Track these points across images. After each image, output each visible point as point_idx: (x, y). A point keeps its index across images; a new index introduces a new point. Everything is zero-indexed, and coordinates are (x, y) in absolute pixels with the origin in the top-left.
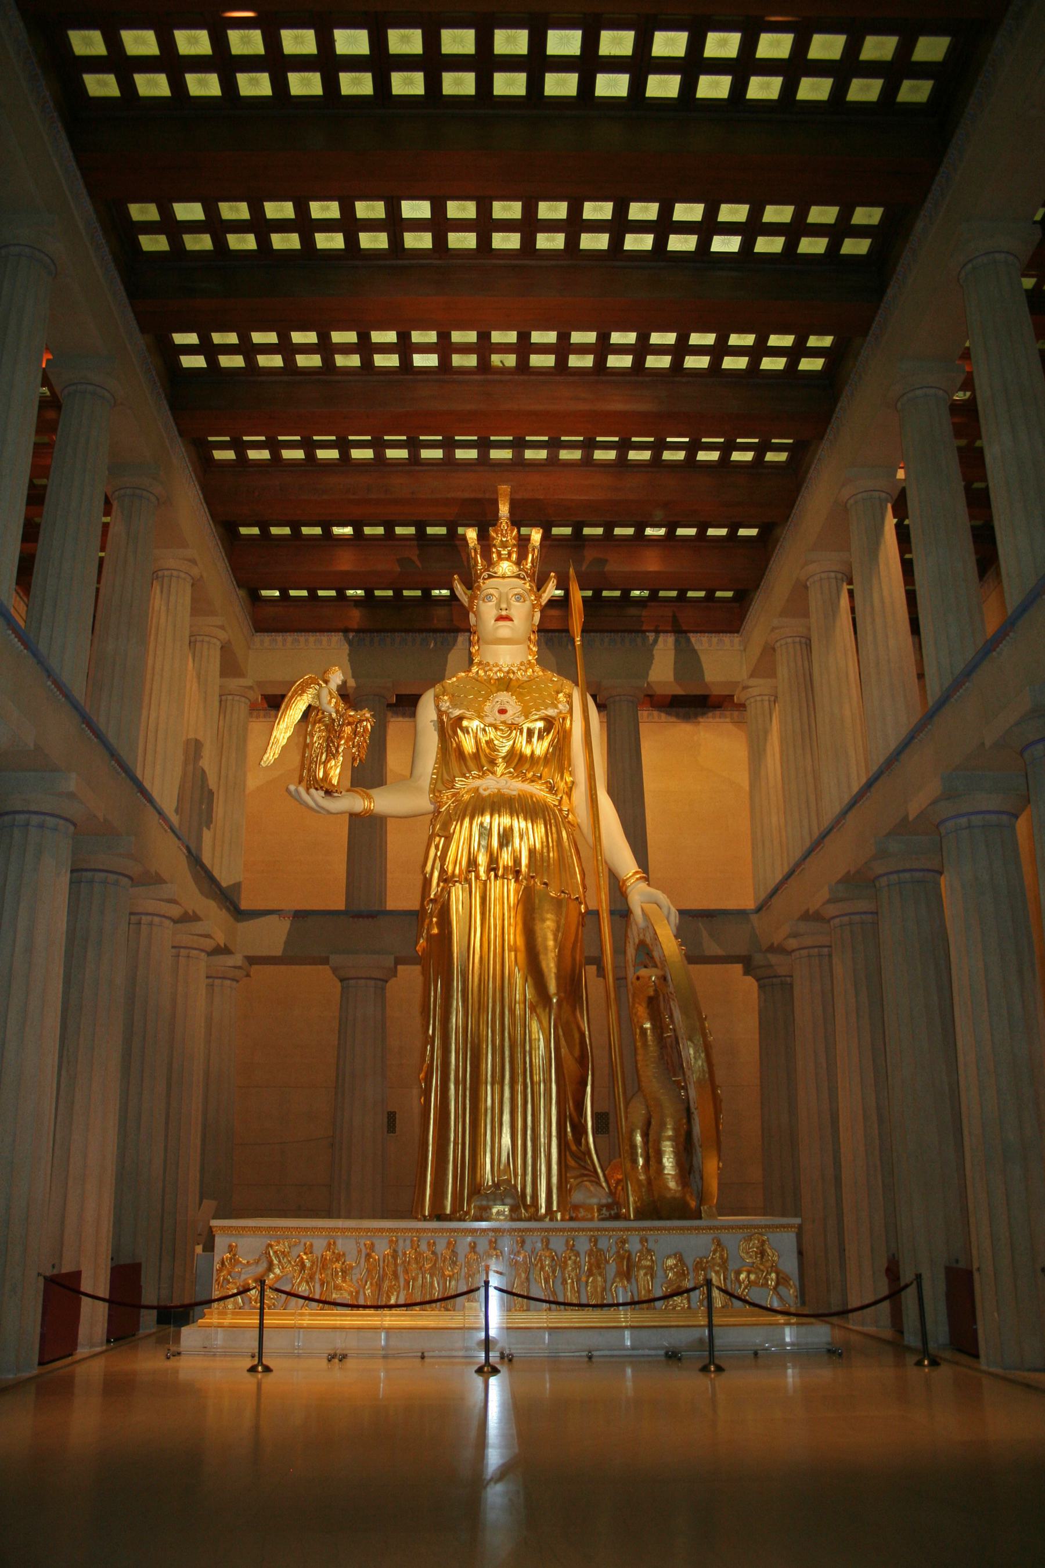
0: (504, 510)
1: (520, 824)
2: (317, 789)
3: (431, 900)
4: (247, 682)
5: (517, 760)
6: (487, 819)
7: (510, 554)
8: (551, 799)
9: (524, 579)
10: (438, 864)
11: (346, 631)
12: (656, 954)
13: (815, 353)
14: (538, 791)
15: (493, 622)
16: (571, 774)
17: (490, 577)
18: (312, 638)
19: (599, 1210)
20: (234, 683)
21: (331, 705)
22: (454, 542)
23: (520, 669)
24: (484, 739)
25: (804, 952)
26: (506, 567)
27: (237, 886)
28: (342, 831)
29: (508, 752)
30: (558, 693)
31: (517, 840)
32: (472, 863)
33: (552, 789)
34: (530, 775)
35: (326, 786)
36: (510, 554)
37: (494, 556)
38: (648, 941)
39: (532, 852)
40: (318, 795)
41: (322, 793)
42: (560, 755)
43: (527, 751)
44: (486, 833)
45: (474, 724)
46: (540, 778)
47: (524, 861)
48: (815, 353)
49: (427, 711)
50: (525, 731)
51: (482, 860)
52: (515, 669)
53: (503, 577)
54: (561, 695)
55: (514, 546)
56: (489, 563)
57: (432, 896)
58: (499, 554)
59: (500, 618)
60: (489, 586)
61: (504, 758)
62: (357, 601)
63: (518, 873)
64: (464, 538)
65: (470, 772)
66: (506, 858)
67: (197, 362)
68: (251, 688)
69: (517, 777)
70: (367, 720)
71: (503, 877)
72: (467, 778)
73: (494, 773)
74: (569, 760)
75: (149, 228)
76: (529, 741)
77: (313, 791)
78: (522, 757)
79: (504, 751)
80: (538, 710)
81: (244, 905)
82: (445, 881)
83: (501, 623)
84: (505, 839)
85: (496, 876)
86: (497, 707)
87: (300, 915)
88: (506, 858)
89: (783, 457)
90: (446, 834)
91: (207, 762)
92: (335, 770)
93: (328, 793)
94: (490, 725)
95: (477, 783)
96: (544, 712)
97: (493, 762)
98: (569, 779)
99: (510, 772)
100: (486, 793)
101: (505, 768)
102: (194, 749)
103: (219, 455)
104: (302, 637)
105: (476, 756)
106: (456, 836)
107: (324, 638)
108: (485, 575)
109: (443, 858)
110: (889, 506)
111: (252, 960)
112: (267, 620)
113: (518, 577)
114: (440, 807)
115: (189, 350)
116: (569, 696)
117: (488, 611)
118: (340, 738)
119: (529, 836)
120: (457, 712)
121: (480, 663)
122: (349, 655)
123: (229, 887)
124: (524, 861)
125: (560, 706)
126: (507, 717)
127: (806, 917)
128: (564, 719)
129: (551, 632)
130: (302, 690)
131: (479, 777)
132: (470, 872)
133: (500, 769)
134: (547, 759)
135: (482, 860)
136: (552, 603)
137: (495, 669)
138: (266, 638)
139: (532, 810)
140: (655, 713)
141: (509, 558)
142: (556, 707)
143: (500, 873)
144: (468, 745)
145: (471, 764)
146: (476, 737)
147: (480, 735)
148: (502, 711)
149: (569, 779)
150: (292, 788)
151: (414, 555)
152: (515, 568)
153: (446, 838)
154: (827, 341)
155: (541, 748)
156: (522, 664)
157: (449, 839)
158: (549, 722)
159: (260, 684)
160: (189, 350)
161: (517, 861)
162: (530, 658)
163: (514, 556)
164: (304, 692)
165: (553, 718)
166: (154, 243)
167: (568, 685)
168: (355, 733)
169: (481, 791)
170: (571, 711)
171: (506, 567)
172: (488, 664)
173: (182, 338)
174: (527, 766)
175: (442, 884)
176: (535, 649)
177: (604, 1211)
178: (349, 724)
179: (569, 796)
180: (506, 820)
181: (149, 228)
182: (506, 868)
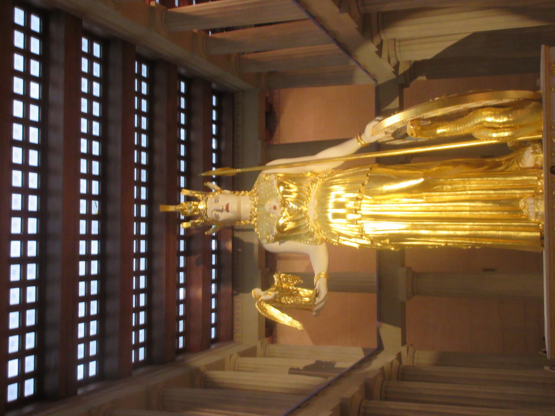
0: (172, 208)
1: (332, 199)
2: (315, 301)
3: (372, 243)
4: (258, 344)
5: (299, 200)
6: (330, 216)
7: (194, 205)
8: (320, 182)
9: (207, 198)
10: (352, 240)
11: (233, 295)
12: (399, 127)
13: (91, 47)
14: (315, 189)
15: (229, 213)
16: (307, 173)
17: (206, 215)
18: (236, 311)
19: (537, 153)
20: (259, 351)
21: (270, 294)
22: (188, 237)
23: (253, 200)
24: (289, 217)
25: (398, 55)
26: (201, 206)
27: (365, 350)
28: (336, 294)
29: (295, 204)
30: (265, 180)
31: (341, 200)
32: (353, 222)
33: (314, 182)
34: (307, 193)
35: (314, 296)
36: (194, 205)
37: (196, 213)
38: (392, 131)
39: (347, 191)
40: (318, 300)
43: (294, 195)
44: (336, 216)
45: (281, 222)
46: (309, 188)
47: (352, 195)
48: (91, 47)
49: (275, 247)
50: (285, 196)
51: (351, 216)
52: (253, 202)
53: (206, 209)
54: (266, 179)
55: (191, 203)
56: (200, 216)
58: (195, 210)
59: (227, 210)
60: (211, 215)
61: (299, 207)
62: (218, 289)
63: (357, 199)
64: (187, 230)
65: (306, 224)
66: (351, 205)
67: (93, 366)
68: (262, 343)
69: (308, 199)
70: (279, 276)
71: (360, 207)
72: (309, 226)
73: (306, 212)
74: (299, 174)
75: (21, 389)
76: (290, 193)
77: (316, 303)
78: (299, 197)
79: (295, 207)
81: (375, 346)
82: (362, 236)
83: (230, 209)
84: (340, 205)
85: (359, 210)
86: (272, 210)
87: (381, 318)
88: (351, 205)
89: (144, 68)
91: (301, 364)
92: (305, 293)
93: (317, 295)
94: (282, 213)
95: (311, 219)
96: (275, 186)
97: (301, 212)
98: (309, 174)
99: (306, 203)
100: (317, 216)
101: (304, 205)
102: (294, 371)
103: (142, 357)
104: (236, 316)
106: (339, 231)
107: (236, 305)
108: (205, 218)
109: (350, 237)
110: (169, 10)
111: (404, 343)
112: (227, 335)
113: (206, 201)
114: (323, 239)
115: (86, 370)
116: (267, 175)
117: (223, 216)
118: (289, 289)
119: (339, 192)
120: (275, 231)
121: (251, 221)
123: (365, 354)
125: (272, 179)
126: (278, 205)
127: (379, 53)
128: (278, 177)
129: (235, 184)
130: (264, 309)
131: (308, 219)
133: (304, 209)
134: (299, 185)
135: (351, 216)
136: (219, 184)
137: (253, 213)
138: (236, 335)
139: (326, 191)
140: (274, 138)
141: (197, 206)
142: (272, 181)
143: (358, 208)
144: (290, 225)
145: (302, 223)
146: (288, 221)
147: (287, 219)
148: (275, 208)
149: (309, 174)
150: (314, 313)
151: (194, 258)
152: (202, 203)
153: (339, 235)
154: (85, 42)
155: (294, 188)
156: (251, 199)
157: (340, 234)
158: (280, 184)
159: (260, 338)
160: (86, 370)
161: (352, 199)
162: (247, 195)
163: (195, 203)
164: (265, 308)
165: (278, 182)
166: (29, 387)
167: (262, 176)
168: (286, 282)
169: (315, 218)
170: (275, 174)
171: (201, 206)
172: (251, 217)
173: (80, 376)
174: (302, 195)
175: (364, 237)
176: (243, 192)
177: (537, 151)
178: (281, 284)
179: (317, 174)
180: (331, 205)
181: (21, 389)
182: (355, 205)
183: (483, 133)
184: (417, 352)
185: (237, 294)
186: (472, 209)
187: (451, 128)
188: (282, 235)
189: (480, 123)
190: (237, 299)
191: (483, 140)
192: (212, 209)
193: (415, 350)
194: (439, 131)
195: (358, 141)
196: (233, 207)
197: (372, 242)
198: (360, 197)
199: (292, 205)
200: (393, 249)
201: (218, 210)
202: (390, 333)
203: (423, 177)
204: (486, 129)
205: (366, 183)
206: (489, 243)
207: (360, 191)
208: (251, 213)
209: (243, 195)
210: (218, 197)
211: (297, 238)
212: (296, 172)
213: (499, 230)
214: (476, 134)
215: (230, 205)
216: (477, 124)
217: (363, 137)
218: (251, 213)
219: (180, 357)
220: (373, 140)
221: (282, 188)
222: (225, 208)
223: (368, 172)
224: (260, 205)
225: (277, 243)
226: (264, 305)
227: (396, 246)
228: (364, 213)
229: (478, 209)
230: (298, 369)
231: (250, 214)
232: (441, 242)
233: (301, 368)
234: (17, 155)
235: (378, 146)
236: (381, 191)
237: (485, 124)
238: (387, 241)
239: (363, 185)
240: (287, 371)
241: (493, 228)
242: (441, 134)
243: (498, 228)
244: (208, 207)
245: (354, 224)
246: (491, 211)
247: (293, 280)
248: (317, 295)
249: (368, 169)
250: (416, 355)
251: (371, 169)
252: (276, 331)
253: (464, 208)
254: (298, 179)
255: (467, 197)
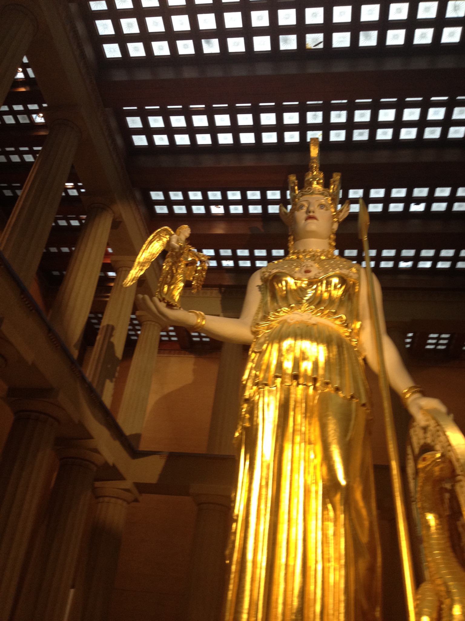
8: (344, 332)
11: (220, 286)
14: (333, 324)
15: (304, 221)
17: (303, 195)
27: (138, 437)
35: (167, 299)
40: (162, 306)
41: (165, 305)
42: (350, 294)
50: (325, 282)
57: (247, 397)
60: (303, 201)
61: (307, 300)
62: (228, 269)
63: (315, 380)
80: (334, 269)
82: (257, 384)
86: (304, 269)
87: (173, 458)
90: (261, 350)
93: (170, 306)
94: (299, 279)
96: (338, 271)
97: (299, 303)
105: (285, 298)
117: (301, 215)
120: (275, 271)
122: (221, 301)
123: (131, 435)
124: (321, 372)
126: (312, 275)
132: (276, 377)
143: (301, 380)
148: (307, 272)
157: (262, 353)
169: (289, 321)
182: (306, 376)
183: (430, 598)
184: (125, 504)
185: (220, 292)
186: (290, 569)
187: (437, 539)
188: (270, 283)
189: (449, 593)
190: (215, 292)
191: (415, 599)
192: (311, 200)
193: (128, 503)
194: (431, 519)
195: (410, 388)
196: (312, 226)
197: (247, 401)
198: (318, 384)
199: (310, 293)
200: (237, 434)
201: (308, 208)
202: (150, 470)
203: (348, 485)
204: (437, 604)
205: (341, 394)
206: (230, 595)
207: (327, 383)
208: (304, 252)
209: (330, 244)
210: (327, 210)
211: (263, 303)
212: (361, 308)
213: (249, 613)
214: (426, 586)
215: (315, 221)
216: (447, 586)
217: (417, 395)
218: (304, 252)
219: (138, 195)
220: (413, 410)
221: (335, 280)
222: (311, 214)
223: (359, 398)
224: (314, 257)
225: (260, 283)
226: (165, 240)
227: (239, 439)
228: (292, 389)
229: (290, 581)
230: (111, 336)
231: (302, 250)
232: (239, 509)
233: (112, 339)
234: (399, 193)
235: (403, 418)
236: (327, 416)
237: (447, 601)
238: (247, 425)
239: (337, 389)
240: (111, 323)
241: (253, 604)
242: (427, 522)
243: (253, 612)
244: (314, 196)
245: (276, 372)
246: (285, 604)
247: (197, 279)
248: (170, 306)
249: (364, 401)
250: (120, 501)
251: (364, 405)
252: (185, 354)
253: (292, 555)
254: (350, 294)
255: (311, 563)
